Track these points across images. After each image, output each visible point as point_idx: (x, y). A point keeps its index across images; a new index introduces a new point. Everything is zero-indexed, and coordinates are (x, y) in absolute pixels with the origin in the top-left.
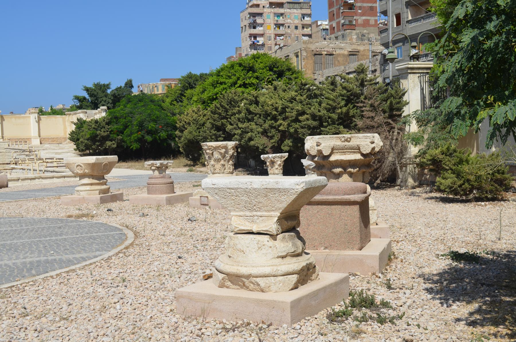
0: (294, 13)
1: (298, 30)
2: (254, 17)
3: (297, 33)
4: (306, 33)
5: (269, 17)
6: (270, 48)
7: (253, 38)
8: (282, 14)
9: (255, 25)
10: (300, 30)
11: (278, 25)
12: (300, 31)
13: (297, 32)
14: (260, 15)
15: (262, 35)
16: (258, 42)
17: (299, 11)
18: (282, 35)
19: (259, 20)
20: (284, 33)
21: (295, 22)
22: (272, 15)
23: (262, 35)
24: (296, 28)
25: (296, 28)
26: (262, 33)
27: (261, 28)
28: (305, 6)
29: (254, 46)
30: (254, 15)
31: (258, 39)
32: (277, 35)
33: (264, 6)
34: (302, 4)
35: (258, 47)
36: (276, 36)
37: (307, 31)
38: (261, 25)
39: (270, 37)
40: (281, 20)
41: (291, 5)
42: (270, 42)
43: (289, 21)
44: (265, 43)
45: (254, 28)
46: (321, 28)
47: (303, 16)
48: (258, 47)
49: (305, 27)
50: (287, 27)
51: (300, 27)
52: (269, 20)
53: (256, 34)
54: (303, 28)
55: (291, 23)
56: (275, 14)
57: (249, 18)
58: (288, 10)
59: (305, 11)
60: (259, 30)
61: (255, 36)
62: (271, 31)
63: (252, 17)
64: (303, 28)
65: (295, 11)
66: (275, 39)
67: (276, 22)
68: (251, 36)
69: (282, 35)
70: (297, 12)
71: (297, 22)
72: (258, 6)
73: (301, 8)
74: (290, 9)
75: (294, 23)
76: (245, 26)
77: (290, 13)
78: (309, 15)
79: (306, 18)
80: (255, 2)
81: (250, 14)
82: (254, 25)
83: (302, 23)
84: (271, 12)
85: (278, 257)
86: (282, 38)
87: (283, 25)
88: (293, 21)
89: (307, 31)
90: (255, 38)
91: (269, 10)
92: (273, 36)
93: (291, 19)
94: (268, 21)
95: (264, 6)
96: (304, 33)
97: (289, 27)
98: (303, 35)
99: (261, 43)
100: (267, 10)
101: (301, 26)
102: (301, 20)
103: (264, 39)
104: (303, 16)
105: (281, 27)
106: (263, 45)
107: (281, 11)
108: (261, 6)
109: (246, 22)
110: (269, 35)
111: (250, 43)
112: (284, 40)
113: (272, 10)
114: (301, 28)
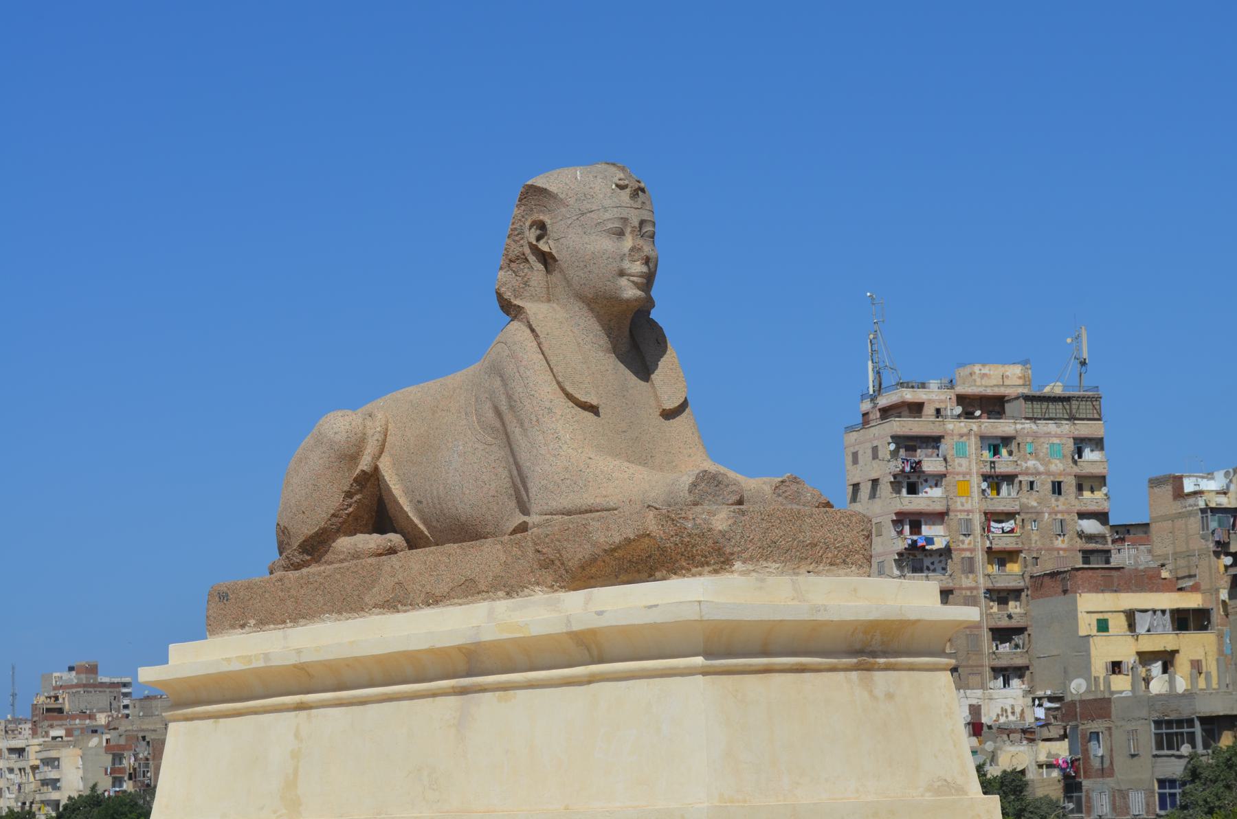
0: (1048, 435)
1: (1062, 499)
2: (911, 449)
3: (1061, 508)
4: (1093, 508)
5: (963, 451)
7: (907, 528)
8: (1007, 440)
9: (914, 479)
10: (1072, 496)
11: (995, 481)
12: (1070, 501)
13: (1060, 503)
14: (933, 441)
15: (939, 517)
16: (930, 541)
17: (1066, 428)
18: (1010, 516)
19: (931, 464)
20: (1017, 508)
21: (1053, 468)
22: (973, 442)
23: (939, 517)
24: (1057, 488)
25: (1057, 488)
26: (939, 507)
27: (936, 492)
28: (1085, 409)
30: (908, 443)
31: (926, 530)
33: (938, 411)
34: (1074, 403)
35: (927, 562)
36: (988, 520)
37: (1093, 499)
38: (938, 479)
39: (969, 521)
40: (1005, 463)
41: (1037, 405)
42: (967, 540)
43: (1031, 463)
44: (953, 546)
45: (912, 489)
46: (1202, 505)
47: (1080, 444)
48: (927, 562)
49: (1086, 485)
50: (1025, 487)
51: (1069, 484)
52: (964, 462)
53: (921, 514)
54: (1080, 488)
55: (1039, 473)
56: (983, 438)
57: (894, 454)
58: (1029, 426)
59: (1085, 429)
60: (930, 498)
61: (915, 521)
62: (971, 501)
63: (902, 452)
64: (1080, 488)
65: (1051, 427)
66: (986, 529)
67: (987, 470)
68: (900, 519)
69: (1010, 516)
70: (1059, 432)
71: (1060, 467)
72: (916, 409)
73: (1072, 418)
74: (1033, 419)
75: (1048, 473)
76: (875, 482)
77: (1036, 436)
78: (1098, 443)
79: (1089, 455)
80: (909, 395)
81: (896, 439)
82: (911, 482)
83: (1076, 470)
84: (968, 434)
86: (1008, 526)
87: (1010, 478)
88: (1046, 464)
89: (1093, 499)
90: (916, 528)
91: (963, 425)
92: (977, 519)
93: (1037, 458)
95: (938, 411)
96: (1084, 509)
97: (1032, 483)
98: (1082, 515)
99: (939, 544)
100: (955, 427)
101: (1074, 482)
102: (1075, 462)
103: (949, 529)
104: (1080, 444)
105: (1004, 488)
106: (946, 552)
107: (1003, 427)
108: (929, 410)
110: (963, 516)
111: (901, 545)
112: (1018, 532)
113: (974, 425)
114: (1074, 489)
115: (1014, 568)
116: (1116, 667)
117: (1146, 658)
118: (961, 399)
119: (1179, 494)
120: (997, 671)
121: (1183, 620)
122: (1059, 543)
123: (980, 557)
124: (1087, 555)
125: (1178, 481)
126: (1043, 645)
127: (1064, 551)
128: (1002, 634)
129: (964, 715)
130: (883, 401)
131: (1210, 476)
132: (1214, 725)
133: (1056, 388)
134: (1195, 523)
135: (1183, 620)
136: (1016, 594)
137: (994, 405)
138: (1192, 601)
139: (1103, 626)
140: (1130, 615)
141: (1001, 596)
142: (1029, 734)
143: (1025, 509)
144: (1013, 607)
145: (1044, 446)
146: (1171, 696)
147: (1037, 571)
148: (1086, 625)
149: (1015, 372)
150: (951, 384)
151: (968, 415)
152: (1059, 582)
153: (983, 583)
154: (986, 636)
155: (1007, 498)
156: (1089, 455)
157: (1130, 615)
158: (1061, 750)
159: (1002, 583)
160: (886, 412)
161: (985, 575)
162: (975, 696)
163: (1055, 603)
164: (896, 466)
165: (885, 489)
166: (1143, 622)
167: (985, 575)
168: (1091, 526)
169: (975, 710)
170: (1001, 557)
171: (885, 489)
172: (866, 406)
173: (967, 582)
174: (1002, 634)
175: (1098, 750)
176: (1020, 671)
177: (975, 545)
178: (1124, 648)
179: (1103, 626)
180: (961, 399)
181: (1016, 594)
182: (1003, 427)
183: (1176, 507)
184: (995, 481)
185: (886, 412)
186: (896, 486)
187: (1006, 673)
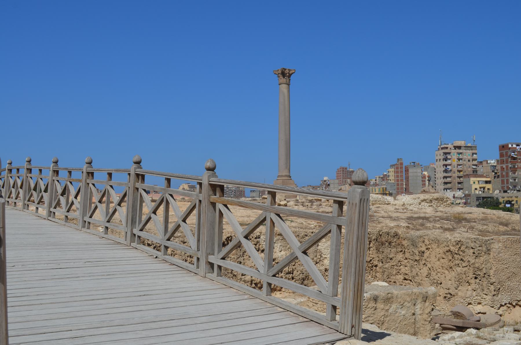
5: (454, 155)
6: (454, 173)
8: (461, 153)
11: (459, 159)
12: (471, 163)
13: (469, 163)
14: (449, 153)
15: (450, 165)
17: (471, 151)
19: (449, 157)
22: (456, 154)
23: (450, 165)
25: (469, 161)
27: (449, 161)
28: (474, 148)
29: (446, 171)
30: (445, 154)
31: (448, 167)
32: (458, 165)
38: (450, 159)
45: (446, 161)
47: (473, 154)
51: (471, 160)
58: (465, 151)
59: (474, 151)
60: (449, 162)
61: (446, 165)
62: (455, 162)
65: (468, 151)
66: (457, 167)
68: (444, 165)
70: (470, 152)
71: (470, 157)
78: (476, 154)
79: (474, 155)
80: (446, 146)
82: (446, 159)
85: (308, 255)
87: (461, 159)
90: (446, 166)
91: (454, 151)
92: (456, 165)
94: (453, 157)
98: (473, 165)
104: (473, 154)
106: (451, 170)
107: (461, 151)
108: (449, 148)
109: (442, 157)
111: (444, 169)
113: (456, 151)
115: (462, 173)
116: (476, 189)
117: (480, 188)
118: (454, 147)
119: (487, 163)
120: (458, 189)
121: (487, 182)
122: (469, 169)
123: (456, 171)
124: (473, 171)
125: (487, 161)
126: (465, 185)
127: (470, 171)
128: (459, 183)
129: (452, 195)
130: (442, 147)
131: (492, 160)
132: (483, 198)
133: (469, 145)
134: (489, 168)
135: (487, 182)
136: (462, 177)
137: (459, 147)
138: (488, 179)
139: (474, 183)
140: (479, 181)
141: (459, 177)
142: (461, 198)
143: (463, 164)
144: (461, 179)
145: (467, 154)
146: (479, 194)
147: (465, 174)
148: (472, 183)
149: (463, 142)
150: (453, 144)
151: (455, 149)
152: (468, 176)
153: (456, 175)
154: (457, 183)
155: (461, 162)
156: (474, 155)
157: (479, 181)
158: (464, 200)
159: (460, 175)
160: (442, 148)
161: (457, 174)
162: (454, 193)
163: (468, 179)
164: (443, 157)
165: (441, 160)
166: (480, 182)
167: (457, 174)
168: (474, 167)
169: (454, 195)
170: (459, 171)
171: (441, 160)
172: (439, 147)
173: (454, 175)
174: (459, 183)
175: (469, 201)
176: (462, 189)
177: (455, 169)
178: (477, 186)
179: (474, 183)
180: (454, 147)
181: (462, 177)
182: (461, 151)
183: (487, 165)
184: (459, 159)
185: (442, 148)
186: (443, 160)
187: (460, 189)
